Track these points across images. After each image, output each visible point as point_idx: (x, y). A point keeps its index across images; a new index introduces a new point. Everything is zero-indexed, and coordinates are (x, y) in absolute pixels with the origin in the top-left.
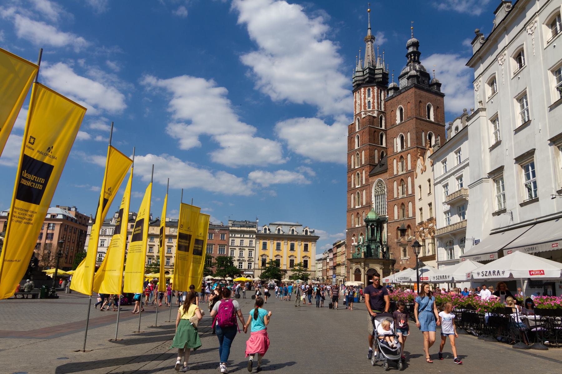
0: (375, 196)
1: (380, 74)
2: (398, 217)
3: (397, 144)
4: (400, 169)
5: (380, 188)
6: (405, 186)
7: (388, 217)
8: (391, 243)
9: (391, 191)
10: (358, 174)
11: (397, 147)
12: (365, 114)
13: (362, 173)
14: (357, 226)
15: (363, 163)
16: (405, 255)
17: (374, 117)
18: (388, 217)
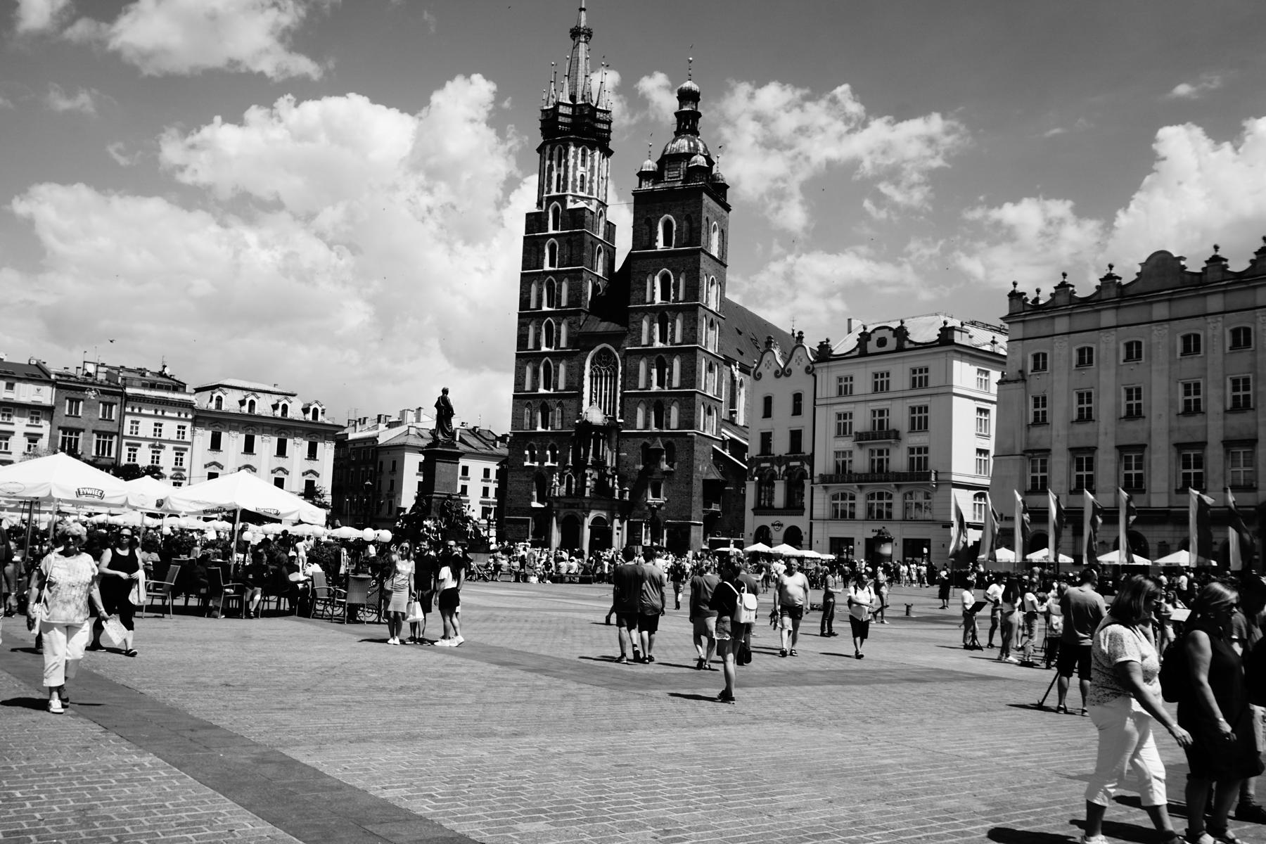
0: (591, 377)
1: (604, 122)
2: (647, 425)
3: (654, 288)
4: (657, 337)
5: (604, 362)
6: (667, 370)
7: (622, 421)
8: (626, 469)
9: (630, 376)
10: (549, 326)
11: (653, 294)
12: (575, 202)
13: (559, 324)
14: (539, 429)
15: (564, 303)
16: (656, 495)
17: (592, 213)
18: (622, 421)
